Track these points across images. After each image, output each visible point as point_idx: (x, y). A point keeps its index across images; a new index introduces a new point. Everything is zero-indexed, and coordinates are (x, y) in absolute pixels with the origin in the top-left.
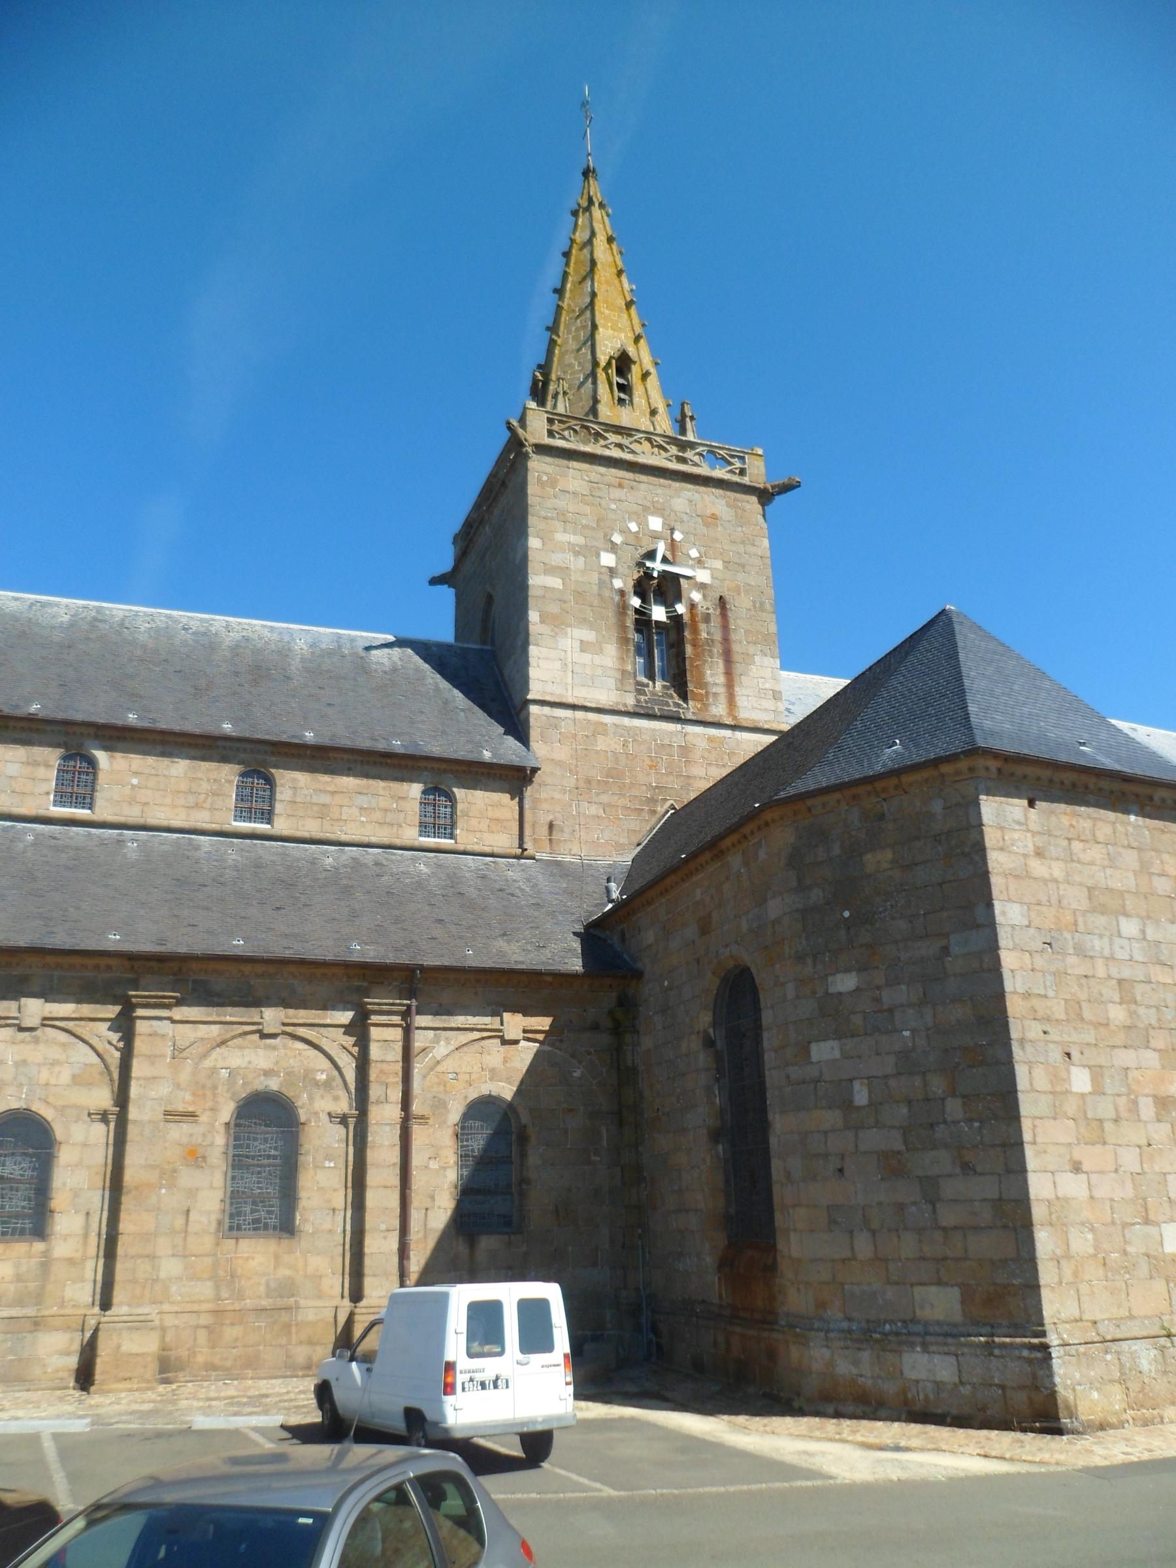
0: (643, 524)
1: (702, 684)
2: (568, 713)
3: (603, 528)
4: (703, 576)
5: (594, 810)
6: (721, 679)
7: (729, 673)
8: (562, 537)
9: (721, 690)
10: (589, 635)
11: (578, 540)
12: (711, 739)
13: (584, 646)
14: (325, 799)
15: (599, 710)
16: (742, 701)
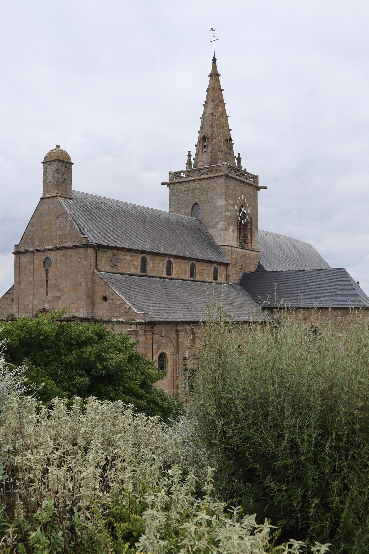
0: (241, 197)
1: (248, 240)
2: (230, 248)
3: (236, 198)
4: (249, 212)
5: (234, 272)
6: (250, 239)
7: (251, 237)
8: (230, 201)
9: (250, 241)
10: (232, 228)
11: (232, 202)
12: (249, 254)
13: (233, 231)
14: (202, 271)
15: (235, 247)
16: (253, 244)
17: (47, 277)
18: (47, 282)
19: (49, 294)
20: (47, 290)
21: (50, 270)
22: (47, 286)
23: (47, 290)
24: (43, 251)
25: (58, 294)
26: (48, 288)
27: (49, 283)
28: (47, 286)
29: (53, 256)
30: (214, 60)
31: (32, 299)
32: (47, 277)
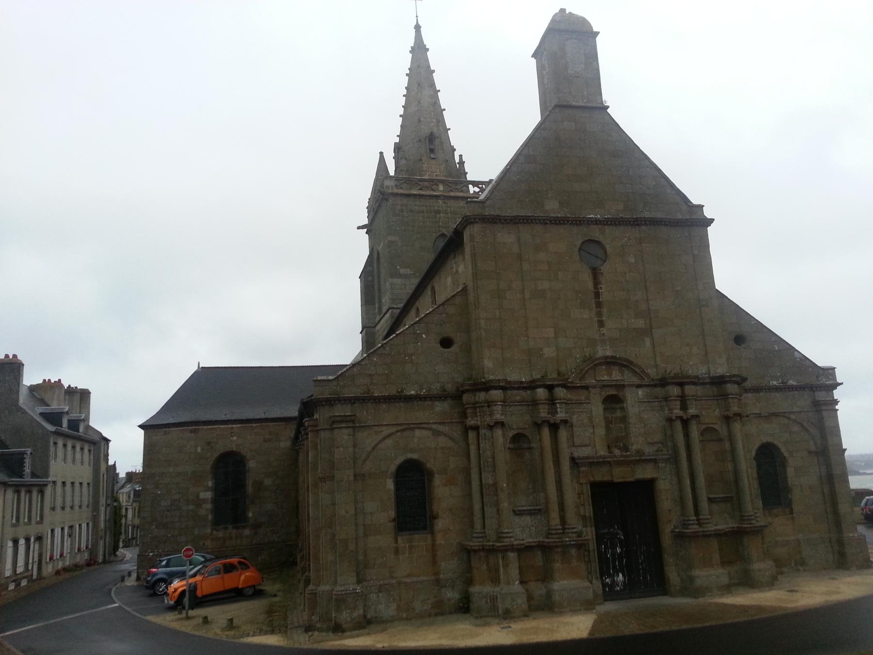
17: (596, 283)
18: (597, 295)
19: (610, 324)
20: (599, 314)
21: (605, 268)
22: (599, 305)
23: (599, 314)
24: (579, 222)
25: (640, 323)
26: (604, 310)
27: (605, 296)
28: (599, 305)
29: (610, 238)
30: (418, 28)
31: (552, 335)
32: (596, 283)
